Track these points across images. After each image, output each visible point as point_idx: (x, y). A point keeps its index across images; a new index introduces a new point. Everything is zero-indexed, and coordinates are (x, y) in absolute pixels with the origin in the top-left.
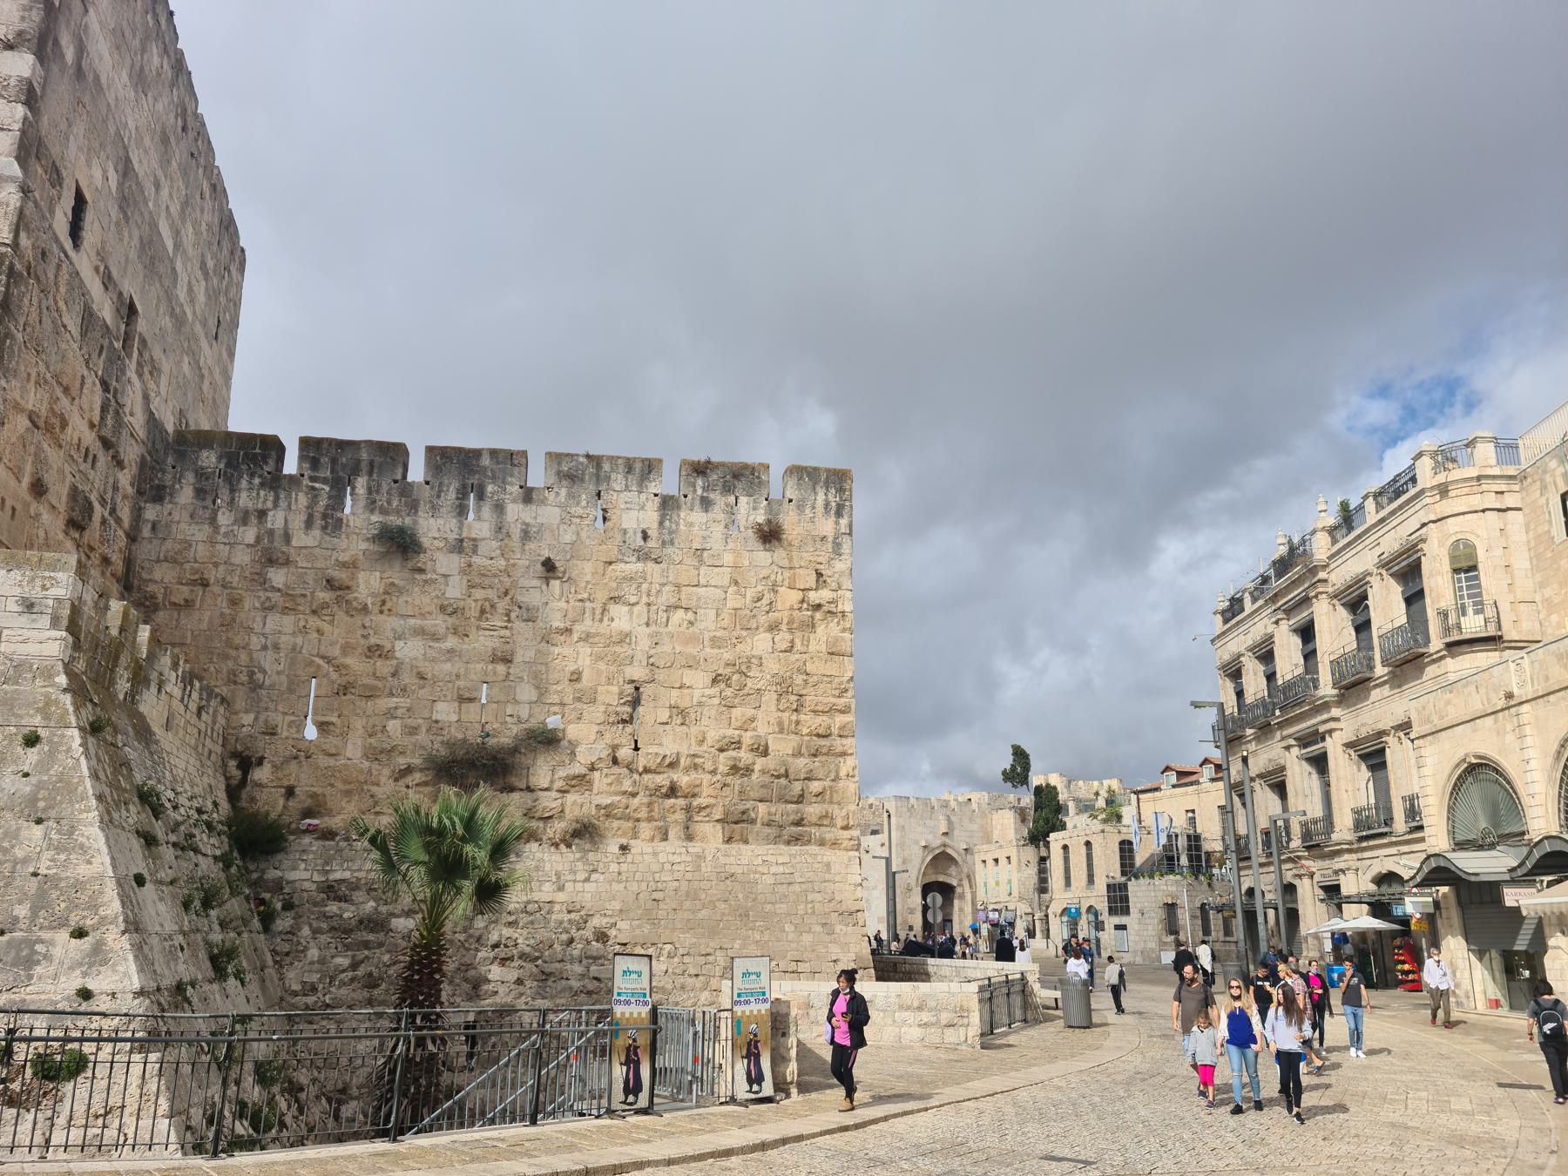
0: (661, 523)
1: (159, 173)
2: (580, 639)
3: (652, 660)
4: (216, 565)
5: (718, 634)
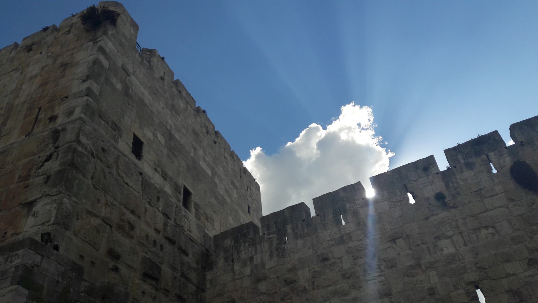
0: (447, 186)
1: (195, 144)
2: (427, 268)
3: (478, 265)
4: (237, 290)
5: (515, 234)
